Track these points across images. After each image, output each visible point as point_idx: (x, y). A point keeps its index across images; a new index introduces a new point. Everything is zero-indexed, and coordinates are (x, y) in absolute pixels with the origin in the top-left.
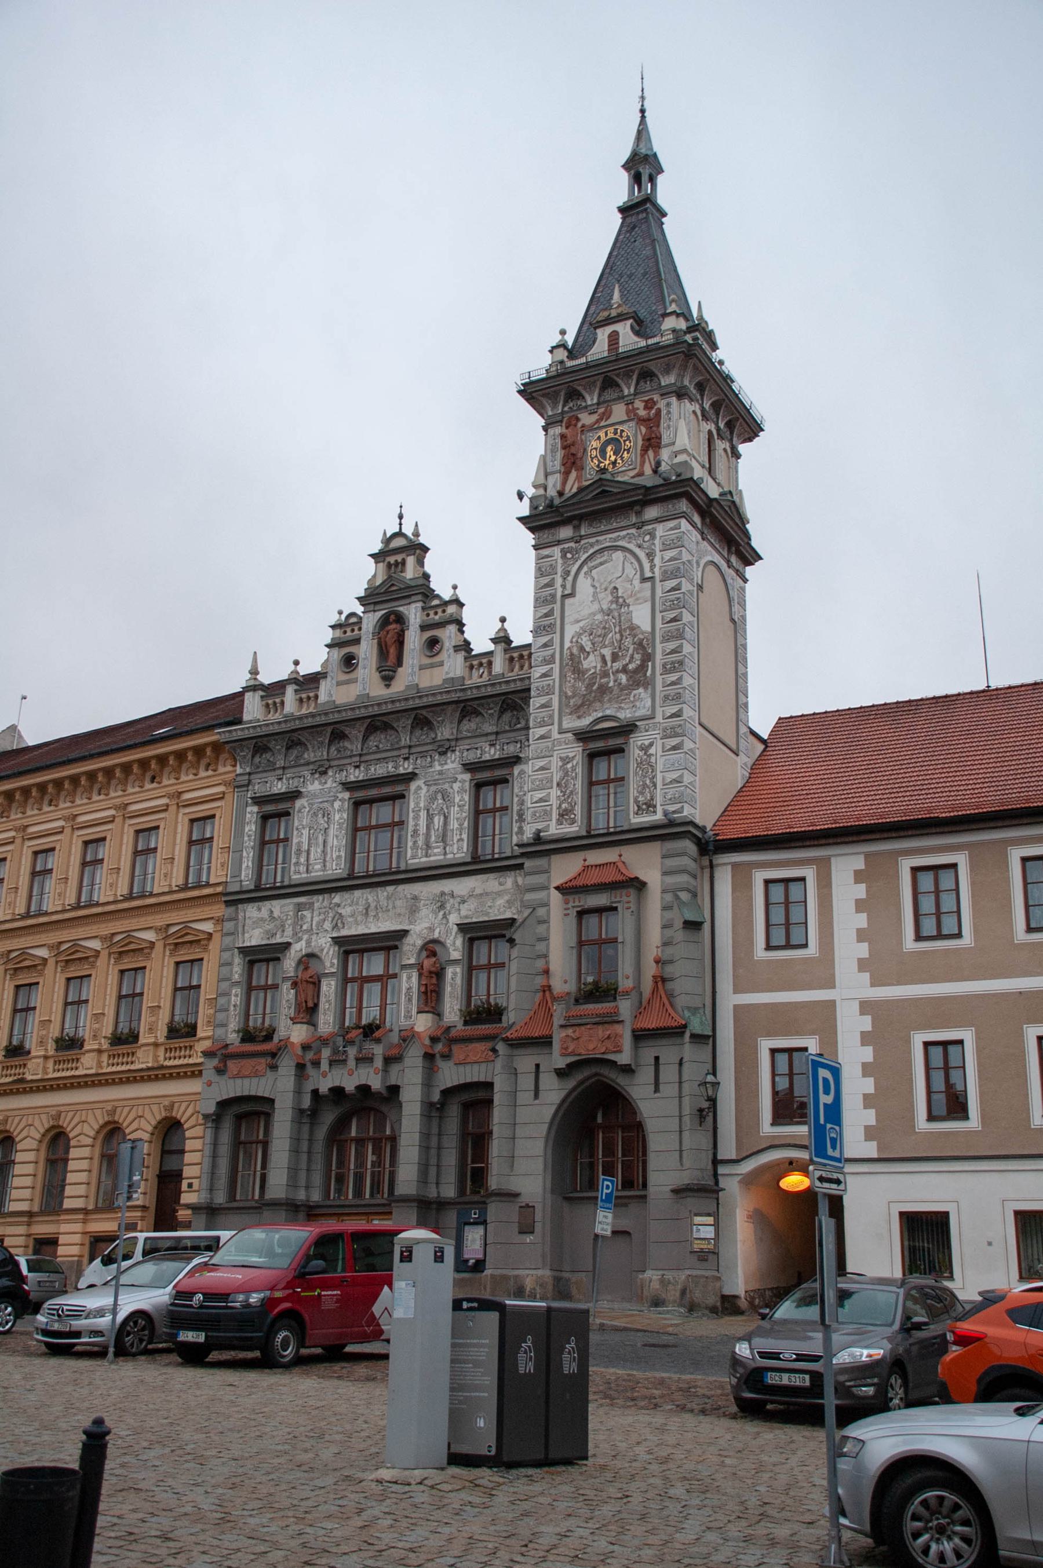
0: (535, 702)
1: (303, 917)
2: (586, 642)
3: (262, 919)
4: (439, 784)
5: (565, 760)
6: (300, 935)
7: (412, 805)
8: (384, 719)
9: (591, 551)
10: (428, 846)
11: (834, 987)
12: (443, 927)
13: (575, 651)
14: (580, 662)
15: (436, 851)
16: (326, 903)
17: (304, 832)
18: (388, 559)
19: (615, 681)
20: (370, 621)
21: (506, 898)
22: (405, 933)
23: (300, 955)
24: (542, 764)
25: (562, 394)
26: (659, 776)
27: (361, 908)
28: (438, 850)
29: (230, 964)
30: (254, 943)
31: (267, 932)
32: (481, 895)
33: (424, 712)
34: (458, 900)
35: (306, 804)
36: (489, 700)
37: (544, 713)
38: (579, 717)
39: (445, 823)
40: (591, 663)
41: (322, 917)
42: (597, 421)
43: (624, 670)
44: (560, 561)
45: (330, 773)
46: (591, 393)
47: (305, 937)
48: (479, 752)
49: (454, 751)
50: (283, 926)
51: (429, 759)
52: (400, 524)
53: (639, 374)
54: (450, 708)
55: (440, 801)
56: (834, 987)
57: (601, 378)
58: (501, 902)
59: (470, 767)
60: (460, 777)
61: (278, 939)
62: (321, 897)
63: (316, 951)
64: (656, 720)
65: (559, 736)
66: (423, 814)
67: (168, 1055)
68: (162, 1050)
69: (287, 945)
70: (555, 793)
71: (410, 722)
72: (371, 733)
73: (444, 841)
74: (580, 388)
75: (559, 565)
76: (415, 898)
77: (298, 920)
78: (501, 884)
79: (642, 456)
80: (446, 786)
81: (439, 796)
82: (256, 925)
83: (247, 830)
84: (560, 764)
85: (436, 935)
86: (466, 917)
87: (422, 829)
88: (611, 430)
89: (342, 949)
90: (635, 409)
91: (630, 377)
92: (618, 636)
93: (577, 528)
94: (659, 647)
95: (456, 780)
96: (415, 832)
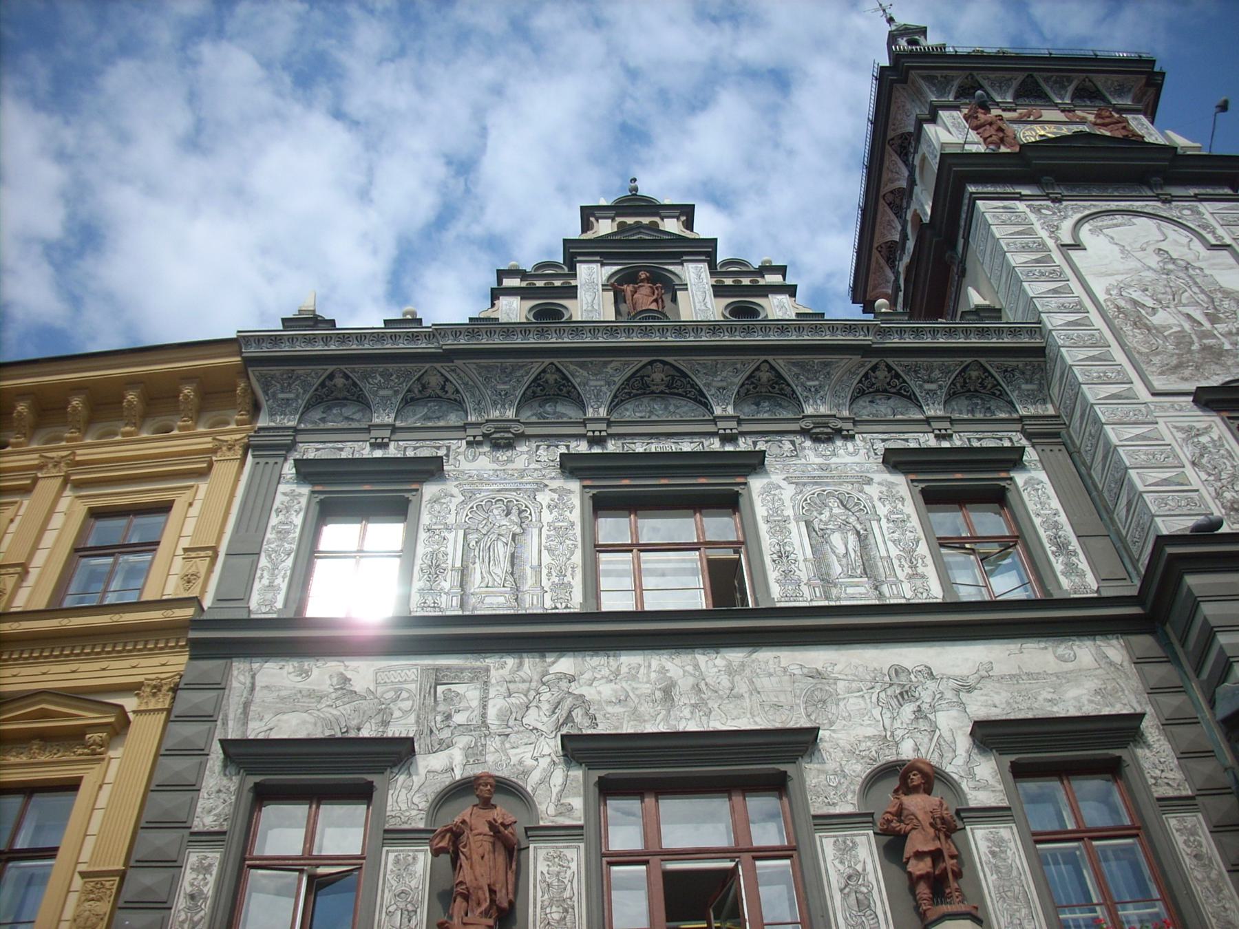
2: (1137, 295)
3: (311, 694)
4: (828, 484)
5: (1192, 434)
6: (445, 734)
7: (761, 511)
8: (681, 362)
9: (1087, 212)
12: (924, 739)
13: (1122, 303)
17: (451, 536)
21: (1092, 684)
22: (802, 742)
23: (446, 780)
25: (956, 83)
27: (646, 689)
28: (862, 590)
29: (193, 788)
31: (329, 724)
32: (1012, 676)
33: (780, 362)
34: (952, 683)
36: (937, 361)
46: (1002, 93)
47: (463, 741)
49: (852, 437)
51: (787, 446)
55: (836, 511)
57: (1021, 77)
59: (896, 461)
60: (877, 477)
62: (510, 661)
63: (504, 773)
69: (397, 753)
71: (738, 380)
72: (631, 396)
76: (817, 675)
78: (1062, 659)
81: (833, 502)
83: (274, 520)
84: (1179, 435)
85: (907, 752)
89: (596, 775)
91: (1064, 88)
92: (1202, 296)
95: (869, 481)
96: (782, 555)
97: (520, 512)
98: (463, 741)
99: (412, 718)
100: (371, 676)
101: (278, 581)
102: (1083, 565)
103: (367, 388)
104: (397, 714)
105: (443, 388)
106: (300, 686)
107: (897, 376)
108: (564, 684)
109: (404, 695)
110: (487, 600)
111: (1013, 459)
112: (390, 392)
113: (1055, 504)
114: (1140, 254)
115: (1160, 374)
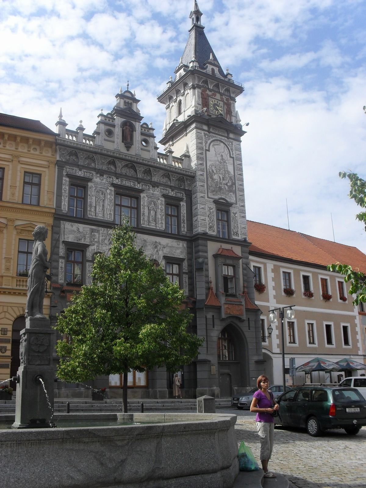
0: (199, 184)
1: (94, 235)
2: (214, 169)
3: (74, 231)
5: (210, 209)
9: (214, 139)
10: (149, 222)
11: (269, 302)
12: (157, 255)
13: (211, 170)
14: (212, 175)
15: (152, 224)
16: (105, 232)
17: (93, 198)
18: (125, 99)
19: (224, 187)
20: (118, 120)
21: (180, 250)
23: (94, 252)
24: (203, 207)
26: (239, 225)
30: (70, 240)
31: (77, 237)
33: (151, 169)
35: (94, 186)
37: (202, 188)
38: (214, 195)
39: (156, 215)
40: (215, 177)
41: (104, 237)
42: (212, 95)
43: (226, 184)
44: (204, 137)
45: (105, 176)
46: (211, 85)
48: (167, 192)
49: (158, 187)
50: (85, 237)
51: (148, 187)
52: (128, 88)
53: (226, 89)
54: (162, 171)
55: (153, 205)
56: (269, 302)
57: (216, 82)
58: (178, 251)
59: (164, 196)
61: (82, 242)
62: (103, 229)
64: (237, 205)
65: (207, 199)
66: (146, 208)
67: (18, 283)
68: (15, 280)
70: (207, 219)
71: (143, 170)
73: (155, 221)
74: (209, 82)
75: (204, 138)
76: (145, 241)
77: (92, 236)
79: (226, 115)
80: (155, 200)
81: (153, 203)
82: (71, 232)
83: (63, 187)
85: (154, 258)
86: (166, 254)
87: (146, 214)
88: (216, 101)
90: (223, 99)
91: (224, 88)
93: (209, 128)
94: (237, 182)
95: (159, 199)
96: (143, 214)
97: (105, 194)
98: (96, 244)
99: (89, 239)
100: (82, 229)
101: (66, 203)
102: (186, 226)
103: (79, 155)
104: (87, 237)
105: (92, 158)
106: (72, 229)
107: (169, 175)
108: (110, 236)
109: (88, 234)
110: (99, 215)
111: (181, 200)
112: (83, 157)
113: (185, 211)
114: (218, 155)
115: (211, 192)
